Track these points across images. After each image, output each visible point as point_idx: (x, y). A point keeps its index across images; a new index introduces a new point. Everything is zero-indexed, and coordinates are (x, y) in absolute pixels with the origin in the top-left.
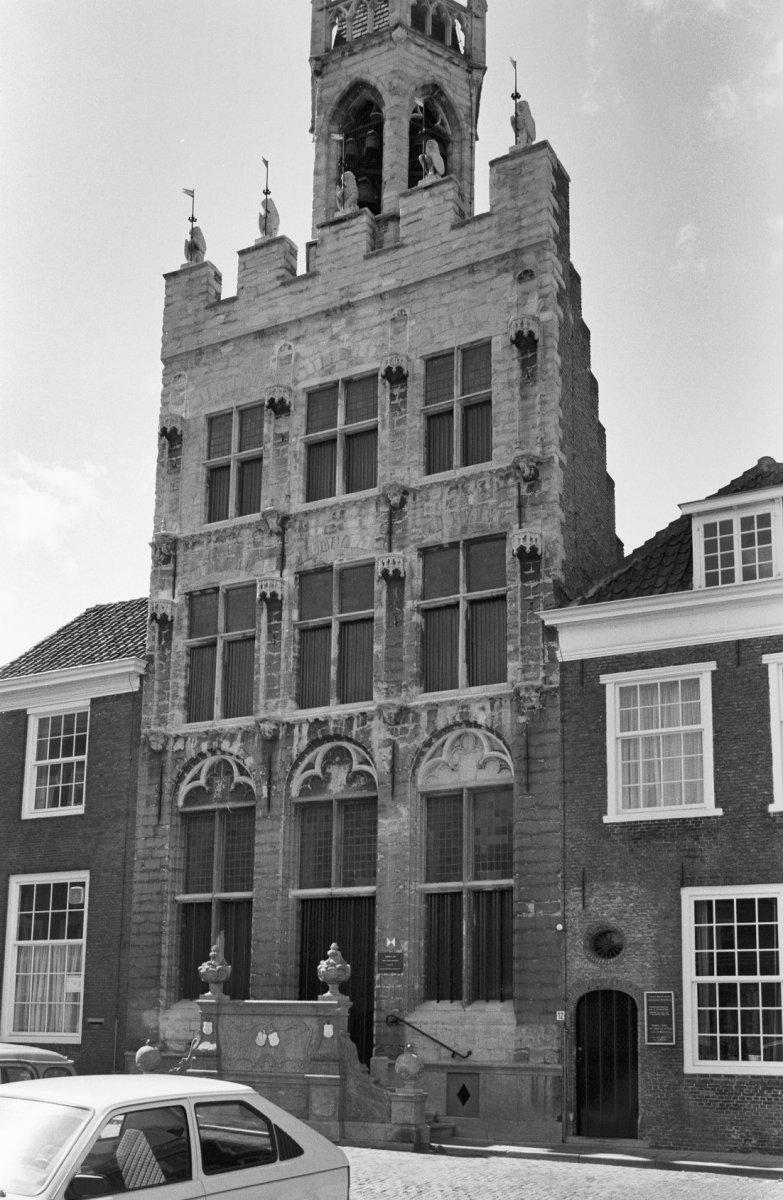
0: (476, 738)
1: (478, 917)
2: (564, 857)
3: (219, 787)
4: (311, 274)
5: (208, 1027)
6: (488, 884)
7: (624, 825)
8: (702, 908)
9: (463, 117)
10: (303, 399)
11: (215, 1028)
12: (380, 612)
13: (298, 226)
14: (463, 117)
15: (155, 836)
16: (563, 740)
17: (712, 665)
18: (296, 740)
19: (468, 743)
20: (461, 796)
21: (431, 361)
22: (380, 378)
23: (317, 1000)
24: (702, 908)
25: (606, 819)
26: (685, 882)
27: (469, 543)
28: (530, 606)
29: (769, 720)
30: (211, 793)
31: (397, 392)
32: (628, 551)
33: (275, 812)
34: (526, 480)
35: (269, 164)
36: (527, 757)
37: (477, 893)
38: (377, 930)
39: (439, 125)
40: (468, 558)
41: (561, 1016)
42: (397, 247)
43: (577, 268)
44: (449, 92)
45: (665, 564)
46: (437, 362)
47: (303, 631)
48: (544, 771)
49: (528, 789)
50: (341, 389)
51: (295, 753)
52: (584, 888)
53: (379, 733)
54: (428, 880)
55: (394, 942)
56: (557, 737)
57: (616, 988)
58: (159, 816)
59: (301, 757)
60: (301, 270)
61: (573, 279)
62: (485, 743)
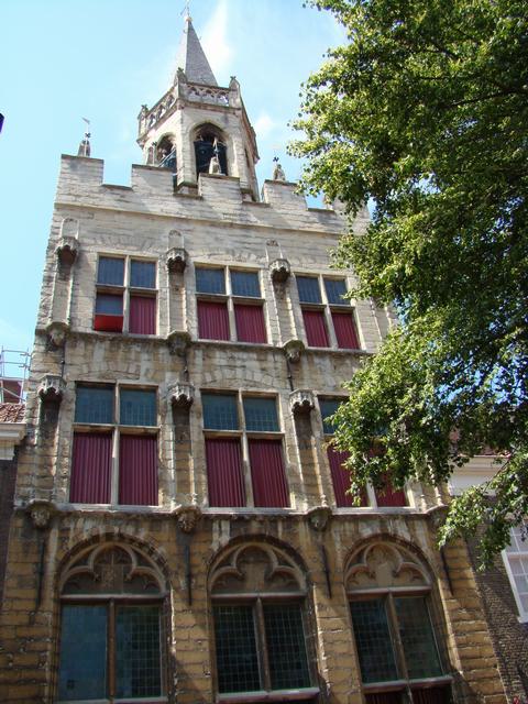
3: (110, 572)
15: (31, 623)
18: (215, 536)
30: (98, 581)
33: (197, 605)
47: (208, 441)
51: (215, 547)
58: (39, 600)
59: (222, 550)
62: (398, 555)
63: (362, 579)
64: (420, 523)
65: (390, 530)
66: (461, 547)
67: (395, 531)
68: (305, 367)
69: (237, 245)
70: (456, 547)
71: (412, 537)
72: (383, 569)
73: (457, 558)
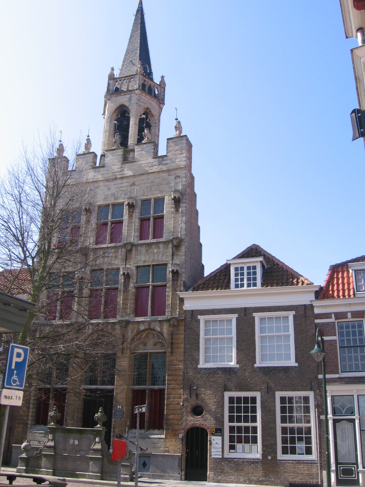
0: (153, 334)
1: (151, 399)
2: (184, 379)
4: (102, 166)
5: (50, 437)
6: (156, 387)
7: (205, 369)
8: (231, 400)
9: (156, 119)
10: (96, 208)
11: (54, 437)
12: (121, 287)
13: (98, 148)
14: (156, 119)
16: (185, 338)
17: (236, 315)
19: (150, 336)
20: (147, 355)
21: (143, 201)
22: (125, 205)
23: (94, 428)
24: (231, 400)
25: (199, 366)
26: (226, 389)
27: (154, 265)
28: (174, 290)
29: (255, 335)
31: (131, 210)
32: (207, 273)
34: (175, 246)
35: (87, 126)
36: (172, 343)
37: (152, 390)
38: (114, 403)
39: (148, 122)
40: (153, 271)
41: (181, 436)
42: (133, 162)
43: (194, 175)
44: (152, 110)
45: (221, 279)
46: (146, 202)
48: (178, 348)
49: (172, 354)
50: (111, 206)
52: (190, 391)
53: (118, 330)
54: (133, 385)
55: (120, 407)
56: (182, 336)
57: (202, 426)
60: (98, 165)
61: (192, 178)
63: (141, 346)
64: (166, 323)
65: (152, 327)
66: (182, 334)
67: (154, 327)
68: (134, 252)
69: (117, 190)
70: (180, 334)
71: (161, 329)
72: (151, 342)
73: (178, 339)
